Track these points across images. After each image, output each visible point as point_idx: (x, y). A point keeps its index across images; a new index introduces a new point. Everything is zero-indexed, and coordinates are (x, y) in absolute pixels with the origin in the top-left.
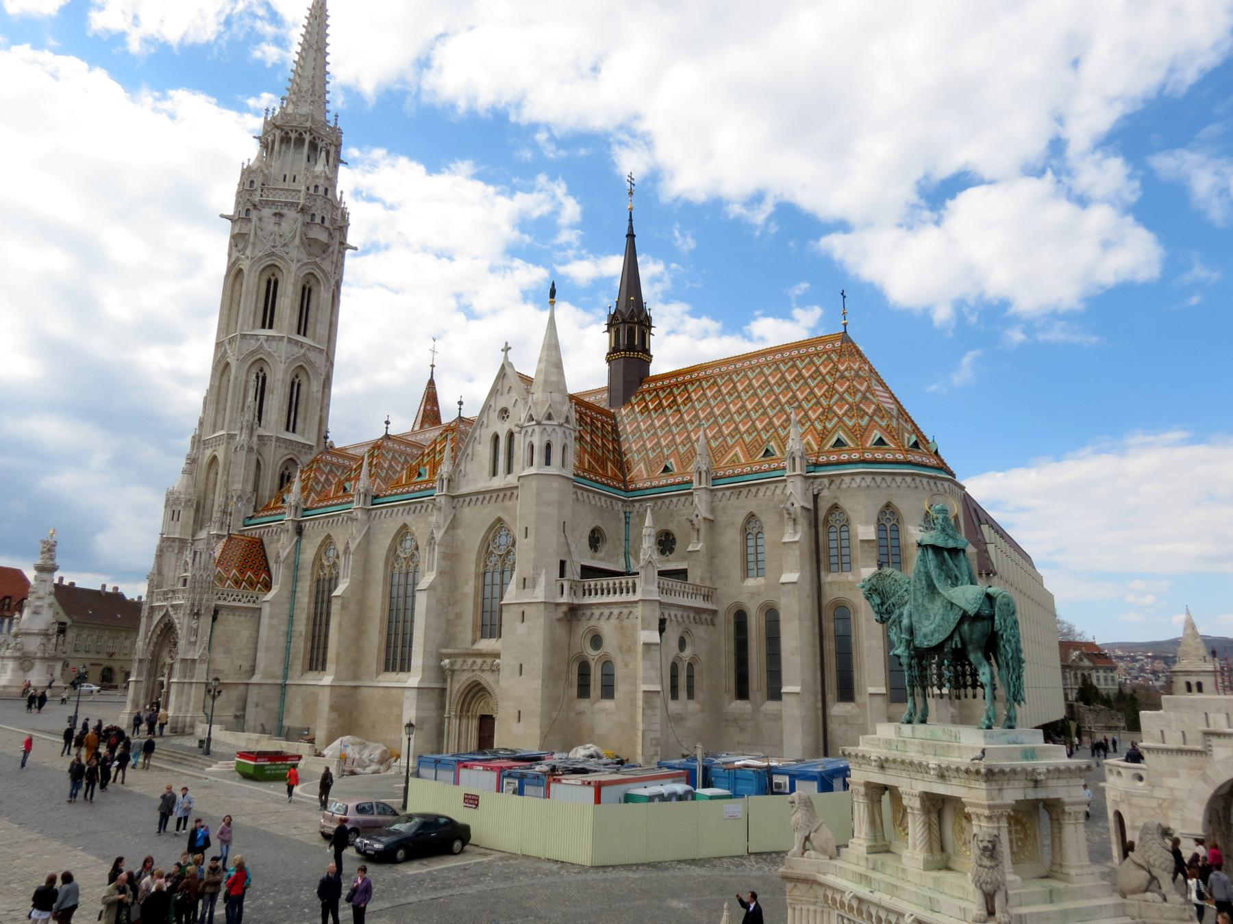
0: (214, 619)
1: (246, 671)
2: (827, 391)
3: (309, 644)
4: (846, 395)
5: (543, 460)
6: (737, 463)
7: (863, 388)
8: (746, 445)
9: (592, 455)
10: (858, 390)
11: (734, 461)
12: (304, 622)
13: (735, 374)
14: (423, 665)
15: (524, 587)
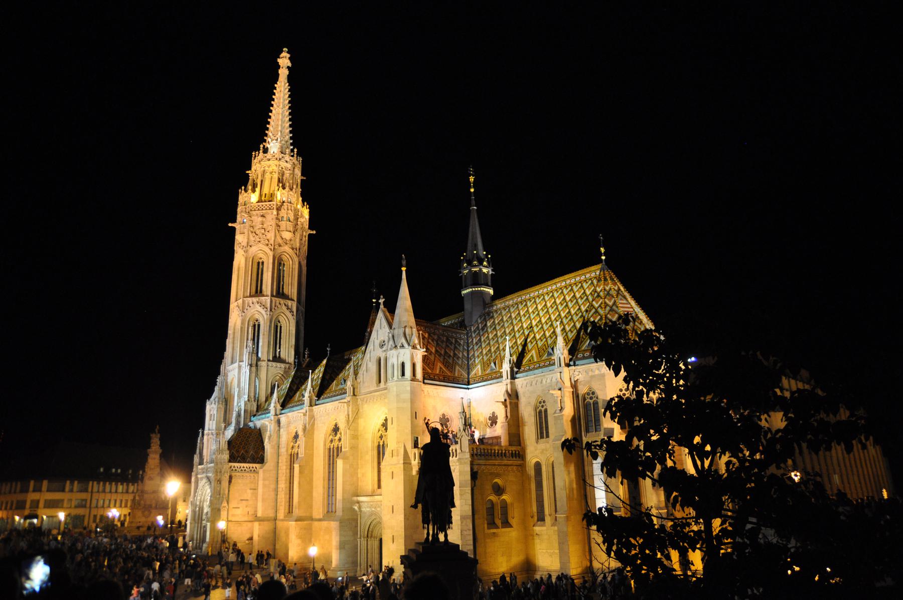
0: (230, 482)
1: (252, 515)
2: (588, 307)
3: (288, 496)
4: (599, 310)
5: (400, 373)
6: (532, 362)
7: (611, 303)
8: (538, 349)
9: (443, 364)
10: (608, 305)
11: (530, 361)
12: (284, 482)
13: (538, 298)
14: (343, 508)
15: (392, 456)
